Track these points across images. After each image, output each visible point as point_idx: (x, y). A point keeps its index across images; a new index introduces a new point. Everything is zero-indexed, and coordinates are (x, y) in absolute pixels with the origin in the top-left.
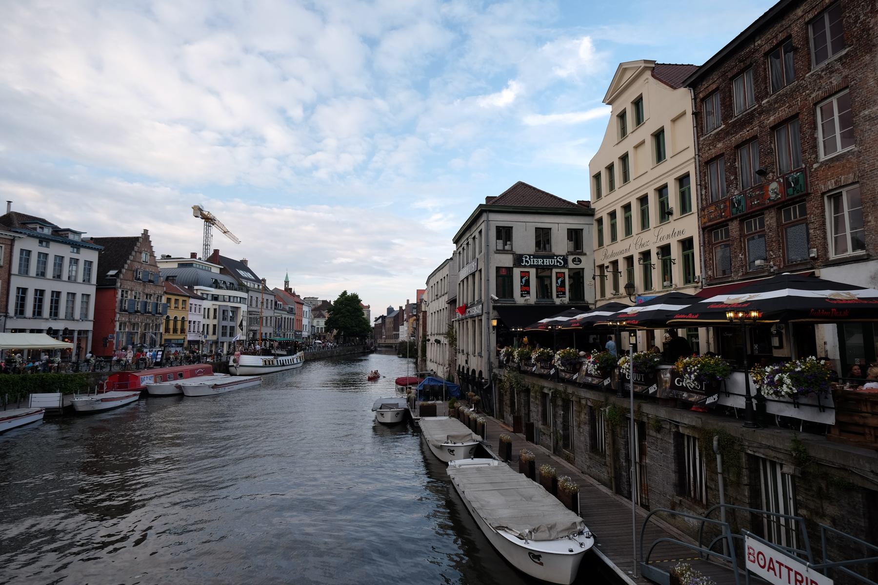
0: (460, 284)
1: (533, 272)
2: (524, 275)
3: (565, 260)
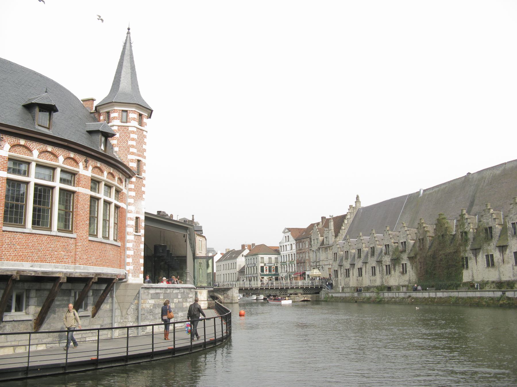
0: (246, 268)
1: (268, 267)
2: (266, 268)
3: (274, 264)
